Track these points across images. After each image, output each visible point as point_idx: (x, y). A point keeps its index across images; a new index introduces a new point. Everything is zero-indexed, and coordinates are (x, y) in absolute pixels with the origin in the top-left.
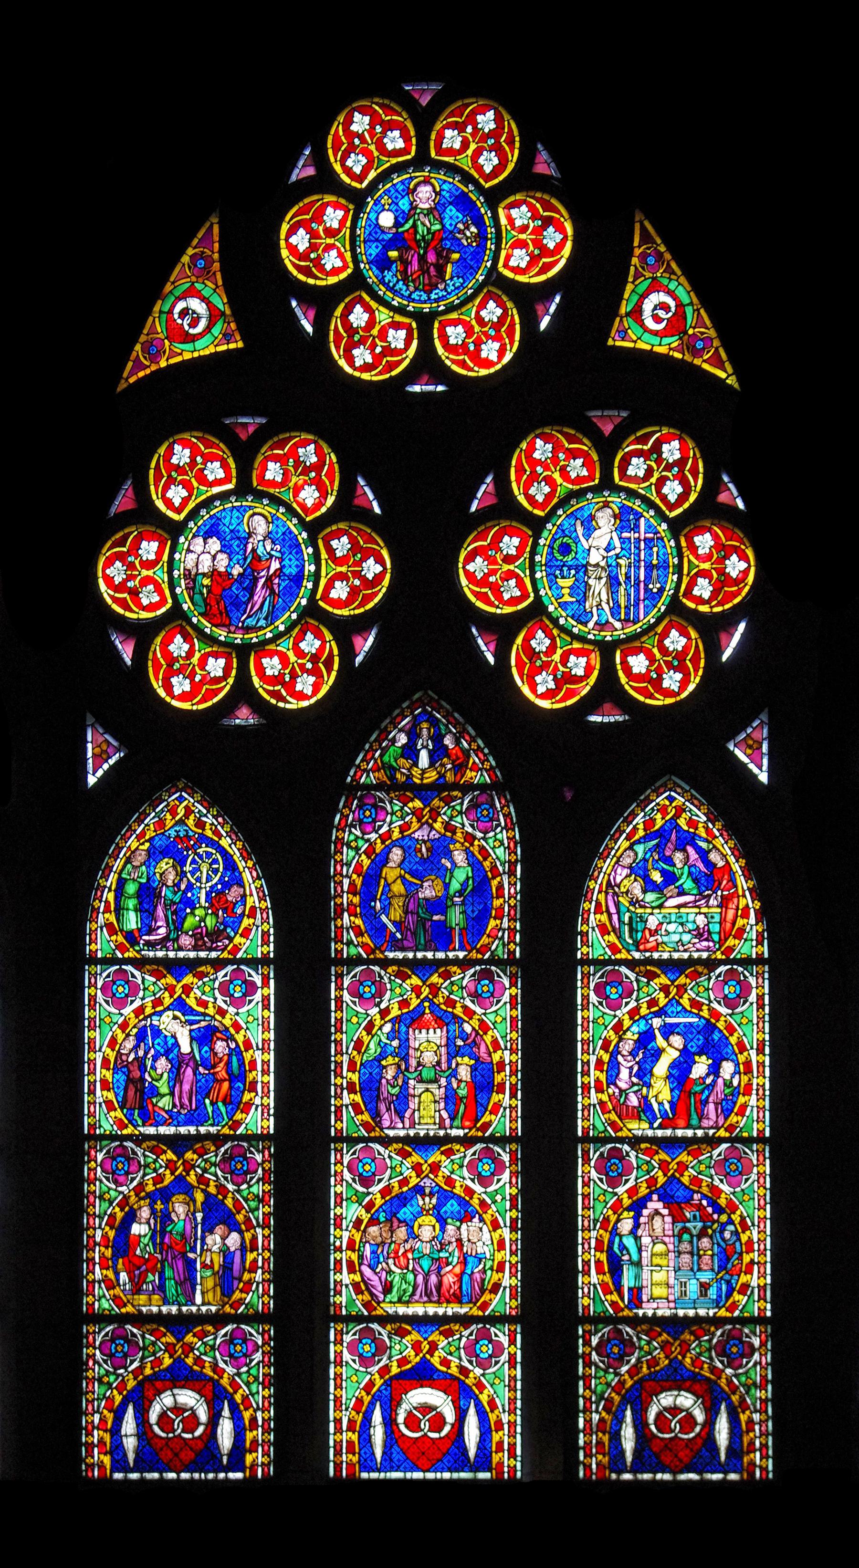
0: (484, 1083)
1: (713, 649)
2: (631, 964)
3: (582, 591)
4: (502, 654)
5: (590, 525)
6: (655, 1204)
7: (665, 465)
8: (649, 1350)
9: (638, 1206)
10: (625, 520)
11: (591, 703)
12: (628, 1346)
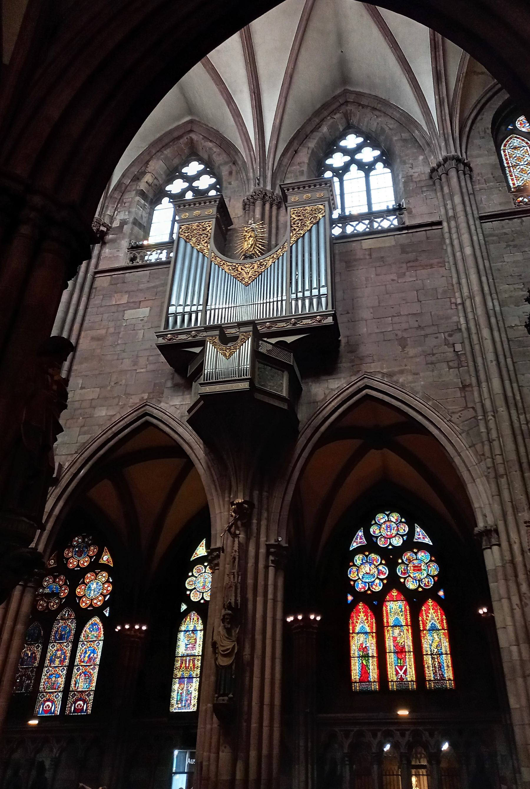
0: (65, 659)
3: (90, 593)
4: (79, 601)
7: (104, 576)
9: (80, 675)
10: (97, 583)
11: (88, 607)
12: (75, 695)
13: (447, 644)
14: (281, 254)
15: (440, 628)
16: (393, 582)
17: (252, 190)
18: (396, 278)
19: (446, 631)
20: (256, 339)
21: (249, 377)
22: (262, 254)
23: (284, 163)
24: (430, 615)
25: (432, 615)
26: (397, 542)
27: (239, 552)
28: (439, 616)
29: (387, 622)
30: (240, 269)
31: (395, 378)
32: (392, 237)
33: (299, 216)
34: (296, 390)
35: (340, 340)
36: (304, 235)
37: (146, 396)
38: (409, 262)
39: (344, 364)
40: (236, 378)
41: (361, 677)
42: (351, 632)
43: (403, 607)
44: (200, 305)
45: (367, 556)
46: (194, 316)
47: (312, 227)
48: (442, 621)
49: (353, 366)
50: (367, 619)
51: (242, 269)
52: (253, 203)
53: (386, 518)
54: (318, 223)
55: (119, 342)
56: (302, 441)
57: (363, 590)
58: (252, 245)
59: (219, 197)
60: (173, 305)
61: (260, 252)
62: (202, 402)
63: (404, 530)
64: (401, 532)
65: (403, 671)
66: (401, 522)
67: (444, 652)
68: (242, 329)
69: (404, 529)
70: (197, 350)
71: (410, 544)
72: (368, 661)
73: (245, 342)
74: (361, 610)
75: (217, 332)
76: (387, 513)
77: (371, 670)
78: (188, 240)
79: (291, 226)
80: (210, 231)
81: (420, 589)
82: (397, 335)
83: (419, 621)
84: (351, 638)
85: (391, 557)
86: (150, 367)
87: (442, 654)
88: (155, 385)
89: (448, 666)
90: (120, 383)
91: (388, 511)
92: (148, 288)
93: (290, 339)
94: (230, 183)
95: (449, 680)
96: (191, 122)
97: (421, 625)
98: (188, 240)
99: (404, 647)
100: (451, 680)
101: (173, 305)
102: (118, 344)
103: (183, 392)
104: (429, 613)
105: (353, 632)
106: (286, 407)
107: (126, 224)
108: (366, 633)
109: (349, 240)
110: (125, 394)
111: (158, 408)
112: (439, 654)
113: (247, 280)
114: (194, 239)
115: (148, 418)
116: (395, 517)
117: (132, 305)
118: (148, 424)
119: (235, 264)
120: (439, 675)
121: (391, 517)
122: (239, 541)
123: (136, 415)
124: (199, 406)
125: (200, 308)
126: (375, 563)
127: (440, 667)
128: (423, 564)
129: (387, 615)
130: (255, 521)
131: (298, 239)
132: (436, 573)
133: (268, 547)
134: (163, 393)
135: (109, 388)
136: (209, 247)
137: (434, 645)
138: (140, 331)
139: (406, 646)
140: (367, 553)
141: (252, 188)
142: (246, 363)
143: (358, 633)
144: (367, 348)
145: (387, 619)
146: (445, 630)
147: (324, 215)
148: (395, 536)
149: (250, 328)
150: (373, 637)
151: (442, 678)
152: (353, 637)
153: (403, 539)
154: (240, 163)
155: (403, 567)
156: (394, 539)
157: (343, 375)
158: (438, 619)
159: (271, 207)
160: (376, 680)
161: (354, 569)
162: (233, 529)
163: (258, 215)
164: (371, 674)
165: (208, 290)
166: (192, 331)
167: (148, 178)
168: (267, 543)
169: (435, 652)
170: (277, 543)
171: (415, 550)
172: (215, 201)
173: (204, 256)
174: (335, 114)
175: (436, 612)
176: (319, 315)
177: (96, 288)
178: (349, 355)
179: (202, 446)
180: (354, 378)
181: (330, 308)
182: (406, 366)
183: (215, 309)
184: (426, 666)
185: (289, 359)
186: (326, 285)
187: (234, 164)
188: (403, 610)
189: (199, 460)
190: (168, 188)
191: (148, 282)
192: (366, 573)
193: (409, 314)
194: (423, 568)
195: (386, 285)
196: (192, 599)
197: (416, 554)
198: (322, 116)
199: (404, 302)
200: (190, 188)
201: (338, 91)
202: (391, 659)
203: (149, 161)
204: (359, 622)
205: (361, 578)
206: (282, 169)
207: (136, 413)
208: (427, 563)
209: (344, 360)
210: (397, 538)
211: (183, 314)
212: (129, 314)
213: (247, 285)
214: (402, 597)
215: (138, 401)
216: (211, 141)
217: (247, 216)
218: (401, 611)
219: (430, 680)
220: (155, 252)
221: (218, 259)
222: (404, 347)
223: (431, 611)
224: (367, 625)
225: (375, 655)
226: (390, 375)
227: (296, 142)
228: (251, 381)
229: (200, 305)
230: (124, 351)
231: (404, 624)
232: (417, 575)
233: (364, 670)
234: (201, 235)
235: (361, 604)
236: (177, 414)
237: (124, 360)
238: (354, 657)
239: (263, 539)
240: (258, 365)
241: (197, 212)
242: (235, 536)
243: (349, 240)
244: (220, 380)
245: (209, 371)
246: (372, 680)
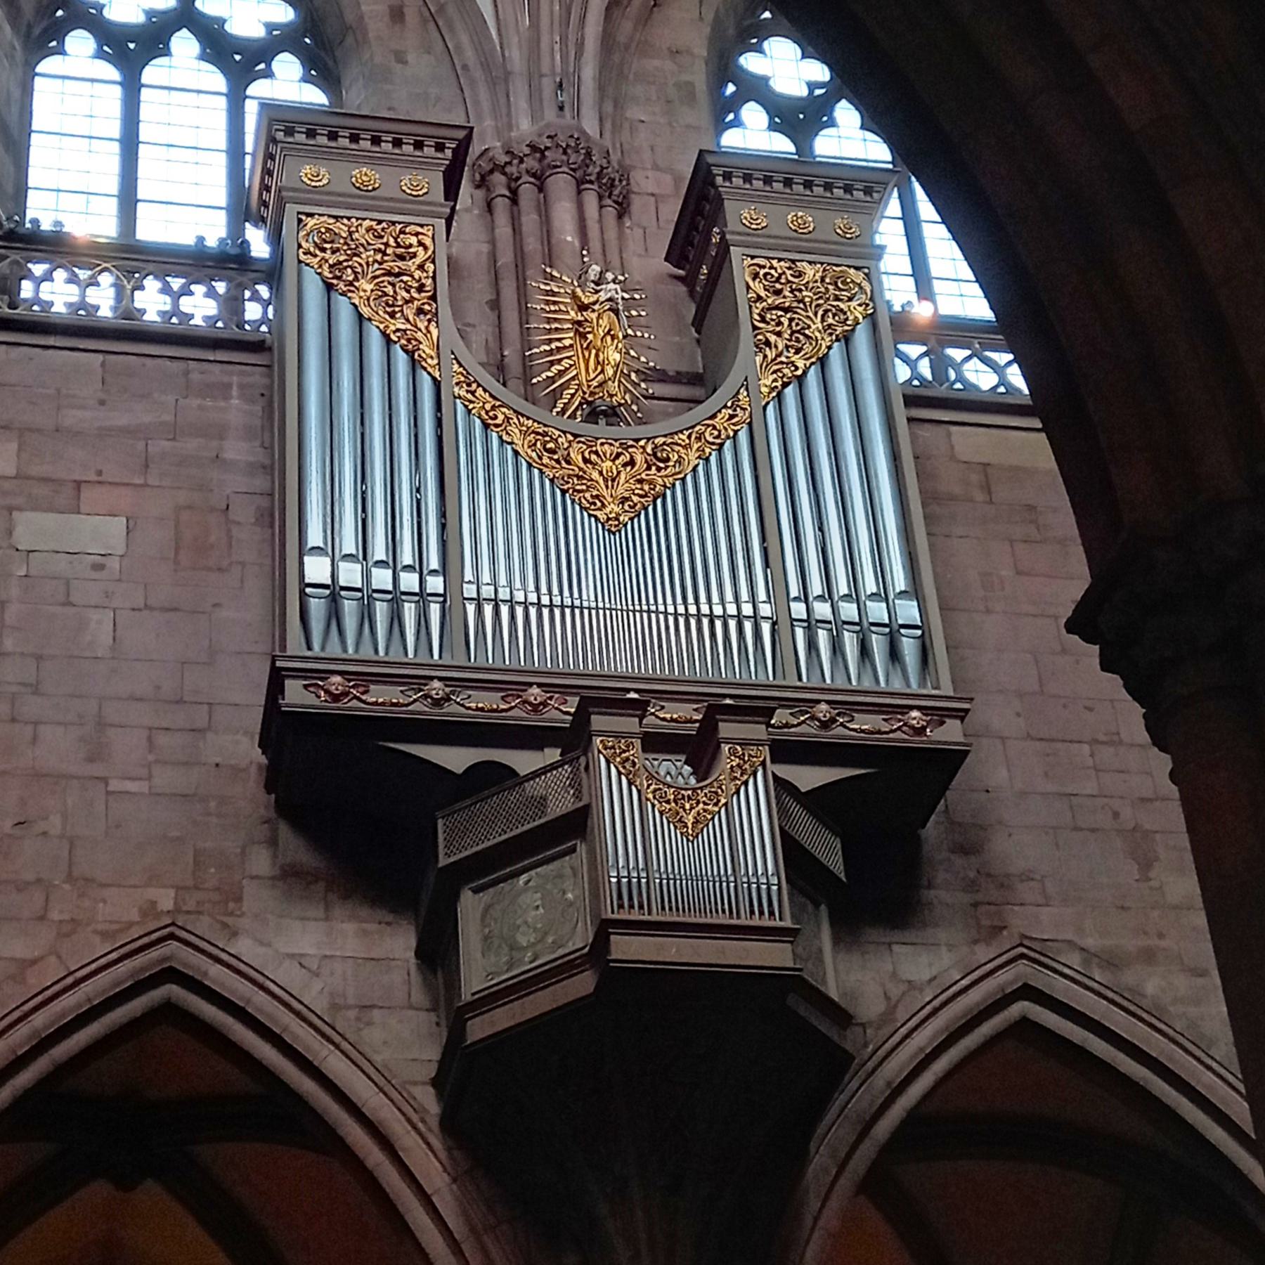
14: (731, 434)
33: (778, 293)
37: (166, 901)
39: (944, 893)
49: (975, 905)
59: (461, 134)
82: (1116, 815)
86: (165, 778)
92: (105, 433)
94: (401, 59)
110: (70, 878)
115: (172, 990)
117: (41, 491)
134: (239, 899)
136: (435, 332)
138: (94, 615)
144: (1017, 847)
157: (942, 935)
176: (919, 708)
178: (959, 861)
179: (436, 1143)
180: (983, 953)
209: (941, 876)
212: (32, 528)
213: (612, 527)
230: (36, 689)
237: (41, 728)
241: (365, 174)
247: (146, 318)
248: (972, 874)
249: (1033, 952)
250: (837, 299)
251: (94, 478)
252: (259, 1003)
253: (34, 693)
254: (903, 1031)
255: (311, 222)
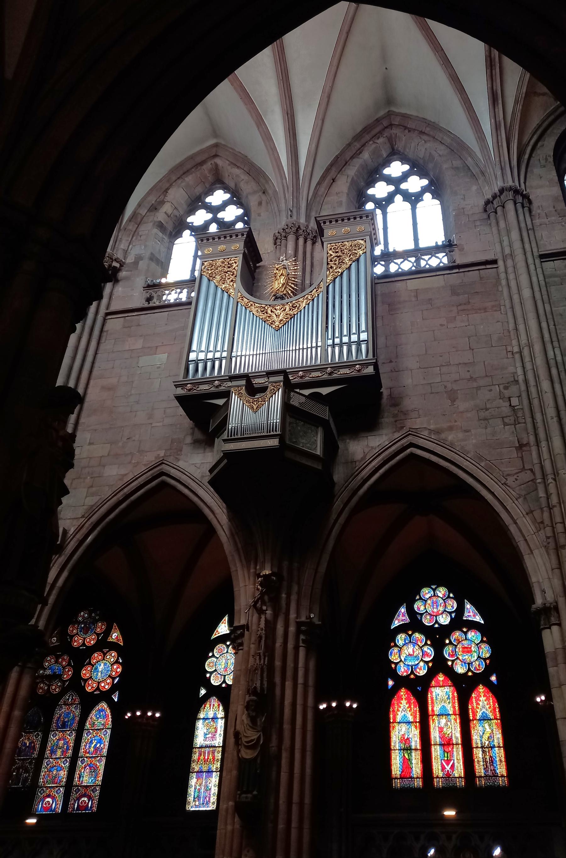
0: (68, 749)
1: (113, 682)
2: (92, 730)
3: (97, 675)
4: (85, 685)
5: (100, 665)
6: (88, 767)
7: (113, 656)
8: (82, 791)
9: (85, 767)
10: (105, 664)
12: (79, 790)
13: (500, 736)
15: (492, 717)
16: (439, 665)
17: (284, 223)
18: (445, 323)
19: (499, 721)
20: (287, 390)
21: (279, 433)
22: (295, 295)
23: (320, 193)
24: (481, 703)
25: (483, 703)
26: (445, 620)
27: (265, 630)
28: (492, 703)
29: (433, 711)
30: (269, 312)
31: (443, 436)
32: (441, 277)
33: (337, 252)
34: (331, 447)
35: (382, 392)
36: (342, 273)
38: (460, 305)
39: (387, 419)
40: (264, 434)
41: (402, 772)
42: (392, 721)
43: (451, 694)
44: (225, 351)
45: (410, 636)
46: (217, 363)
47: (351, 265)
48: (494, 709)
49: (396, 421)
50: (410, 707)
51: (272, 311)
52: (285, 237)
53: (432, 593)
54: (358, 260)
55: (133, 392)
56: (338, 504)
57: (405, 674)
58: (283, 285)
59: (248, 230)
60: (194, 351)
61: (292, 292)
62: (225, 461)
63: (453, 607)
64: (449, 609)
65: (450, 766)
66: (449, 597)
67: (496, 745)
68: (272, 379)
69: (452, 605)
70: (220, 402)
71: (459, 622)
72: (410, 754)
73: (275, 393)
74: (404, 697)
75: (243, 382)
76: (434, 587)
77: (414, 765)
78: (211, 278)
79: (328, 264)
80: (236, 268)
81: (470, 674)
82: (445, 387)
83: (468, 709)
84: (391, 729)
85: (438, 636)
87: (494, 747)
88: (173, 441)
89: (501, 761)
90: (134, 438)
91: (434, 585)
93: (325, 391)
94: (259, 215)
95: (502, 776)
96: (216, 145)
97: (471, 713)
98: (211, 278)
99: (451, 739)
100: (504, 777)
101: (194, 351)
102: (131, 395)
103: (205, 449)
104: (480, 701)
105: (394, 722)
106: (320, 468)
107: (142, 260)
108: (409, 723)
109: (393, 279)
111: (175, 467)
112: (491, 747)
113: (277, 323)
114: (218, 277)
115: (164, 478)
116: (442, 592)
118: (164, 483)
119: (264, 306)
120: (491, 770)
121: (438, 592)
122: (266, 618)
123: (151, 475)
124: (222, 465)
125: (225, 354)
126: (419, 643)
127: (492, 762)
128: (473, 646)
129: (432, 703)
130: (284, 596)
131: (335, 279)
132: (488, 655)
133: (299, 624)
134: (181, 451)
135: (120, 444)
136: (235, 286)
137: (486, 736)
139: (454, 738)
140: (410, 633)
141: (283, 221)
142: (276, 418)
143: (399, 723)
145: (433, 707)
146: (497, 719)
147: (365, 251)
148: (442, 613)
149: (281, 378)
150: (416, 727)
151: (495, 775)
152: (394, 727)
153: (451, 617)
154: (270, 192)
155: (451, 649)
156: (441, 616)
157: (384, 431)
158: (490, 708)
159: (305, 242)
160: (420, 776)
161: (396, 650)
162: (259, 605)
163: (290, 251)
164: (414, 769)
165: (234, 335)
166: (215, 381)
167: (167, 208)
168: (298, 620)
169: (486, 744)
170: (308, 620)
171: (465, 630)
172: (243, 235)
173: (229, 296)
174: (378, 139)
175: (488, 699)
176: (359, 364)
177: (107, 331)
179: (225, 511)
180: (397, 435)
181: (371, 356)
182: (456, 421)
183: (241, 356)
184: (476, 760)
185: (324, 412)
186: (367, 330)
187: (264, 193)
188: (451, 696)
189: (222, 526)
190: (189, 220)
191: (166, 324)
192: (409, 655)
193: (460, 364)
194: (473, 649)
195: (434, 331)
196: (212, 682)
197: (466, 633)
198: (363, 141)
199: (454, 350)
200: (215, 220)
201: (382, 113)
202: (436, 752)
203: (168, 189)
204: (400, 709)
205: (403, 660)
206: (318, 199)
207: (151, 472)
208: (477, 644)
209: (386, 414)
210: (444, 616)
211: (205, 361)
212: (144, 361)
213: (278, 329)
214: (450, 682)
215: (154, 459)
216: (238, 167)
217: (278, 252)
218: (448, 698)
219: (481, 777)
220: (174, 291)
221: (245, 299)
222: (453, 401)
223: (482, 698)
224: (410, 713)
225: (419, 747)
226: (438, 432)
227: (334, 169)
228: (281, 437)
229: (225, 351)
230: (137, 402)
231: (451, 712)
232: (466, 657)
233: (406, 764)
234: (226, 272)
235: (403, 690)
236: (197, 474)
238: (394, 750)
239: (293, 616)
240: (288, 419)
241: (221, 247)
242: (261, 612)
243: (393, 279)
244: (246, 436)
245: (234, 425)
246: (415, 776)
247: (183, 300)
248: (396, 412)
249: (413, 432)
250: (355, 250)
251: (161, 344)
252: (184, 478)
253: (138, 403)
254: (368, 462)
255: (206, 263)
